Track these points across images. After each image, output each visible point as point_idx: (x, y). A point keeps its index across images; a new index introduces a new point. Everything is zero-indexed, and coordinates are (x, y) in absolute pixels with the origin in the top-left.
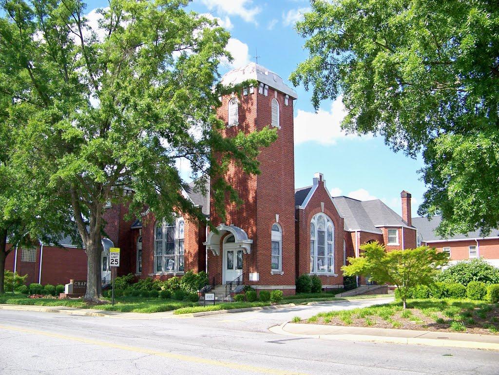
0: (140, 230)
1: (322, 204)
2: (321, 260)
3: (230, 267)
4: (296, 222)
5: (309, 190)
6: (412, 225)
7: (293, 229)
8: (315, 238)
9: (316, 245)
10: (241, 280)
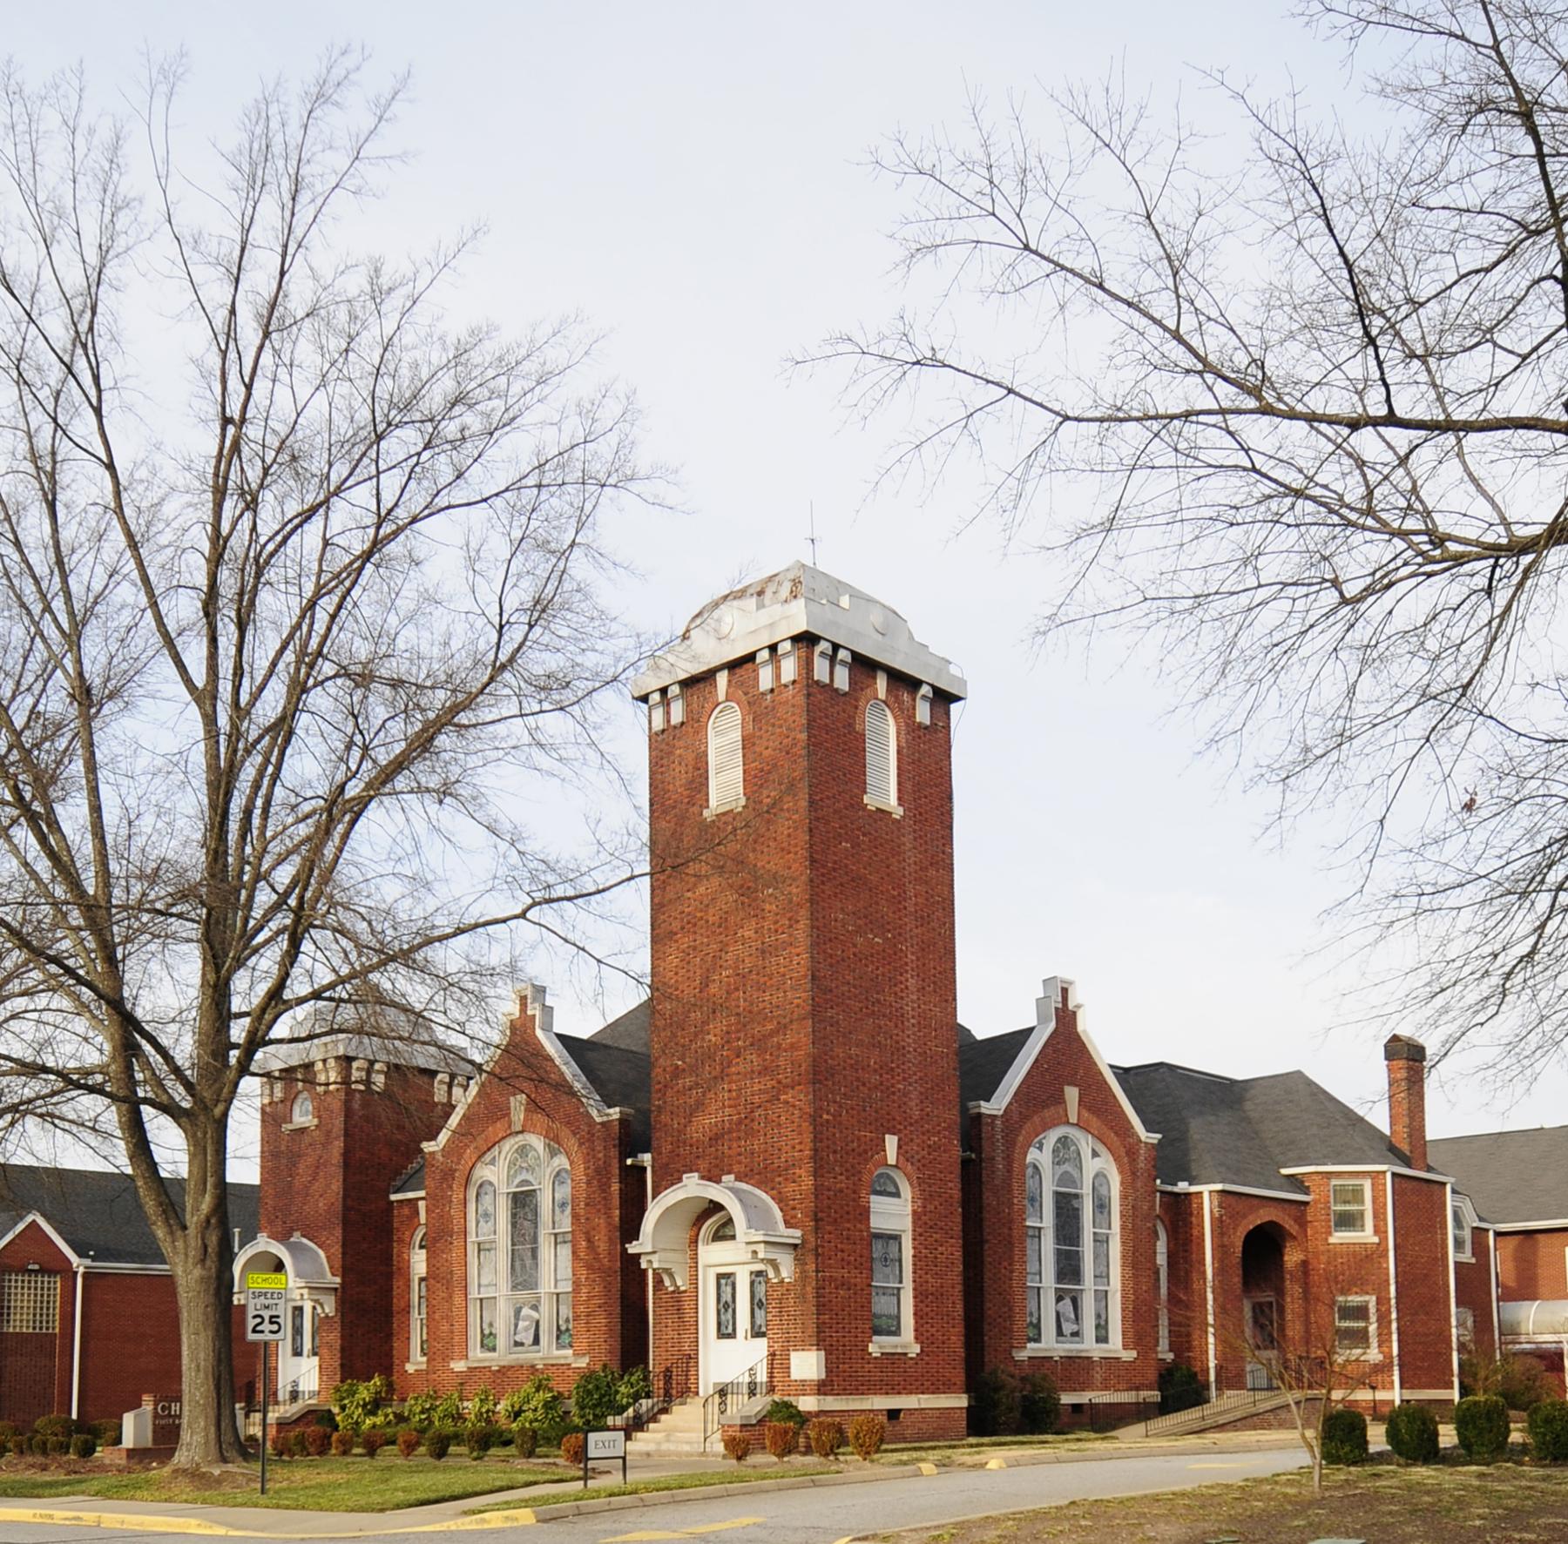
0: (422, 1204)
1: (1072, 1094)
2: (1068, 1301)
3: (726, 1332)
4: (965, 1163)
5: (1023, 1035)
6: (1430, 1161)
7: (954, 1189)
8: (1046, 1220)
9: (1048, 1244)
10: (762, 1377)
